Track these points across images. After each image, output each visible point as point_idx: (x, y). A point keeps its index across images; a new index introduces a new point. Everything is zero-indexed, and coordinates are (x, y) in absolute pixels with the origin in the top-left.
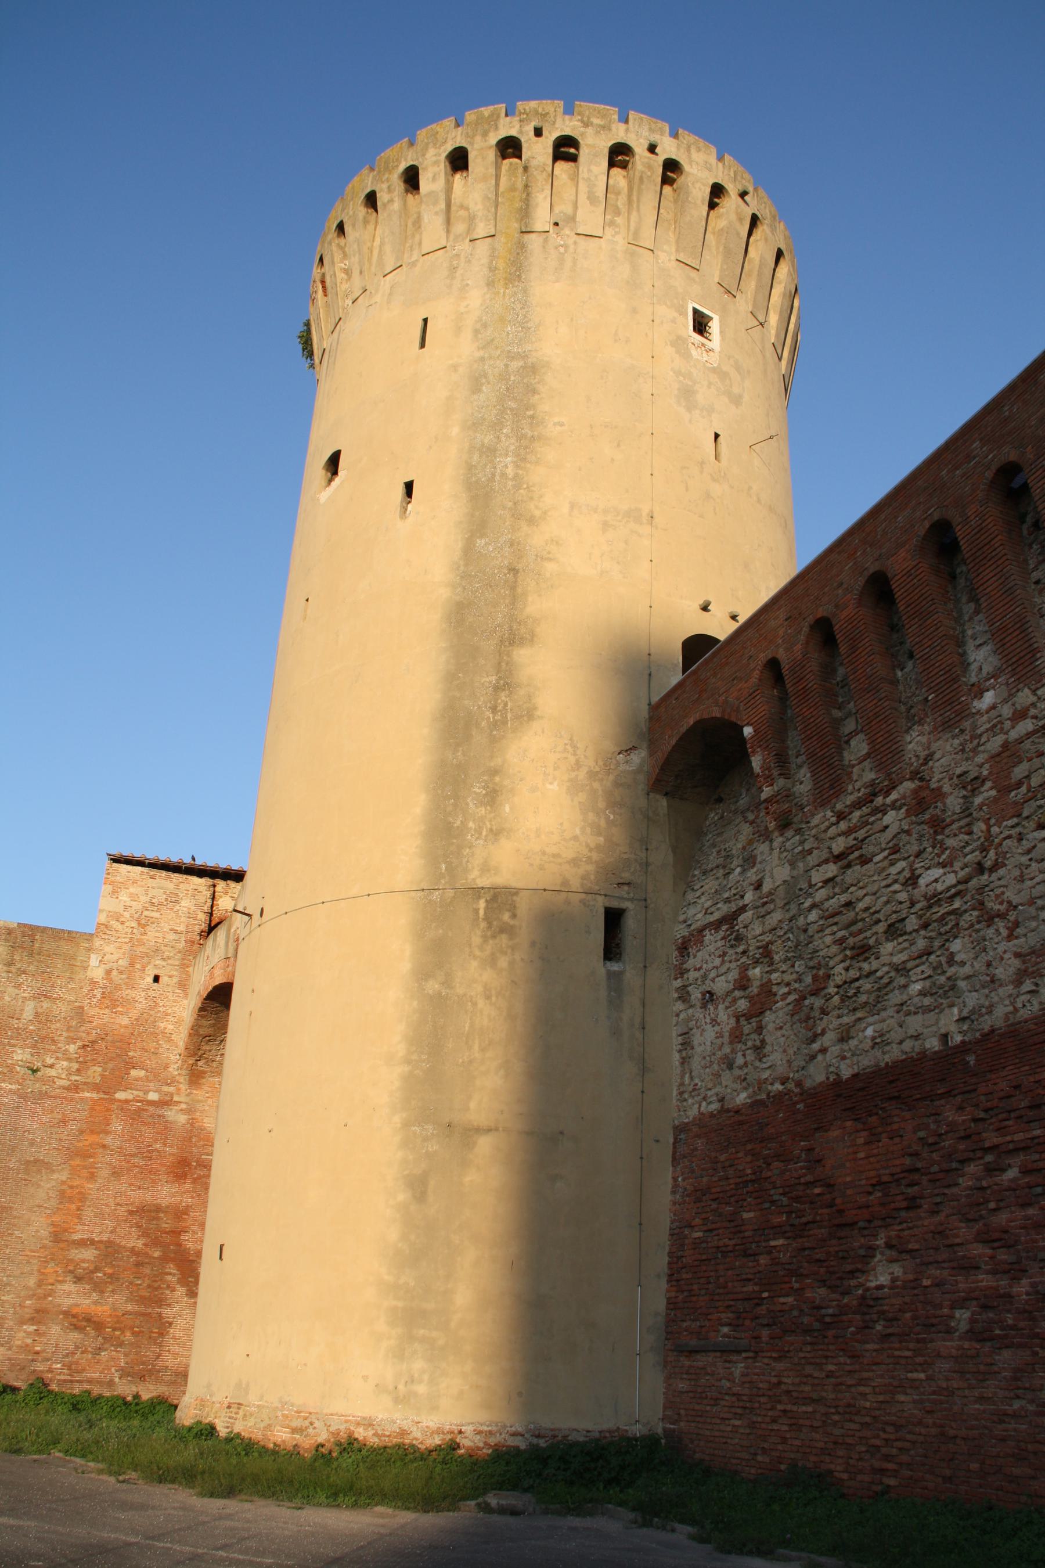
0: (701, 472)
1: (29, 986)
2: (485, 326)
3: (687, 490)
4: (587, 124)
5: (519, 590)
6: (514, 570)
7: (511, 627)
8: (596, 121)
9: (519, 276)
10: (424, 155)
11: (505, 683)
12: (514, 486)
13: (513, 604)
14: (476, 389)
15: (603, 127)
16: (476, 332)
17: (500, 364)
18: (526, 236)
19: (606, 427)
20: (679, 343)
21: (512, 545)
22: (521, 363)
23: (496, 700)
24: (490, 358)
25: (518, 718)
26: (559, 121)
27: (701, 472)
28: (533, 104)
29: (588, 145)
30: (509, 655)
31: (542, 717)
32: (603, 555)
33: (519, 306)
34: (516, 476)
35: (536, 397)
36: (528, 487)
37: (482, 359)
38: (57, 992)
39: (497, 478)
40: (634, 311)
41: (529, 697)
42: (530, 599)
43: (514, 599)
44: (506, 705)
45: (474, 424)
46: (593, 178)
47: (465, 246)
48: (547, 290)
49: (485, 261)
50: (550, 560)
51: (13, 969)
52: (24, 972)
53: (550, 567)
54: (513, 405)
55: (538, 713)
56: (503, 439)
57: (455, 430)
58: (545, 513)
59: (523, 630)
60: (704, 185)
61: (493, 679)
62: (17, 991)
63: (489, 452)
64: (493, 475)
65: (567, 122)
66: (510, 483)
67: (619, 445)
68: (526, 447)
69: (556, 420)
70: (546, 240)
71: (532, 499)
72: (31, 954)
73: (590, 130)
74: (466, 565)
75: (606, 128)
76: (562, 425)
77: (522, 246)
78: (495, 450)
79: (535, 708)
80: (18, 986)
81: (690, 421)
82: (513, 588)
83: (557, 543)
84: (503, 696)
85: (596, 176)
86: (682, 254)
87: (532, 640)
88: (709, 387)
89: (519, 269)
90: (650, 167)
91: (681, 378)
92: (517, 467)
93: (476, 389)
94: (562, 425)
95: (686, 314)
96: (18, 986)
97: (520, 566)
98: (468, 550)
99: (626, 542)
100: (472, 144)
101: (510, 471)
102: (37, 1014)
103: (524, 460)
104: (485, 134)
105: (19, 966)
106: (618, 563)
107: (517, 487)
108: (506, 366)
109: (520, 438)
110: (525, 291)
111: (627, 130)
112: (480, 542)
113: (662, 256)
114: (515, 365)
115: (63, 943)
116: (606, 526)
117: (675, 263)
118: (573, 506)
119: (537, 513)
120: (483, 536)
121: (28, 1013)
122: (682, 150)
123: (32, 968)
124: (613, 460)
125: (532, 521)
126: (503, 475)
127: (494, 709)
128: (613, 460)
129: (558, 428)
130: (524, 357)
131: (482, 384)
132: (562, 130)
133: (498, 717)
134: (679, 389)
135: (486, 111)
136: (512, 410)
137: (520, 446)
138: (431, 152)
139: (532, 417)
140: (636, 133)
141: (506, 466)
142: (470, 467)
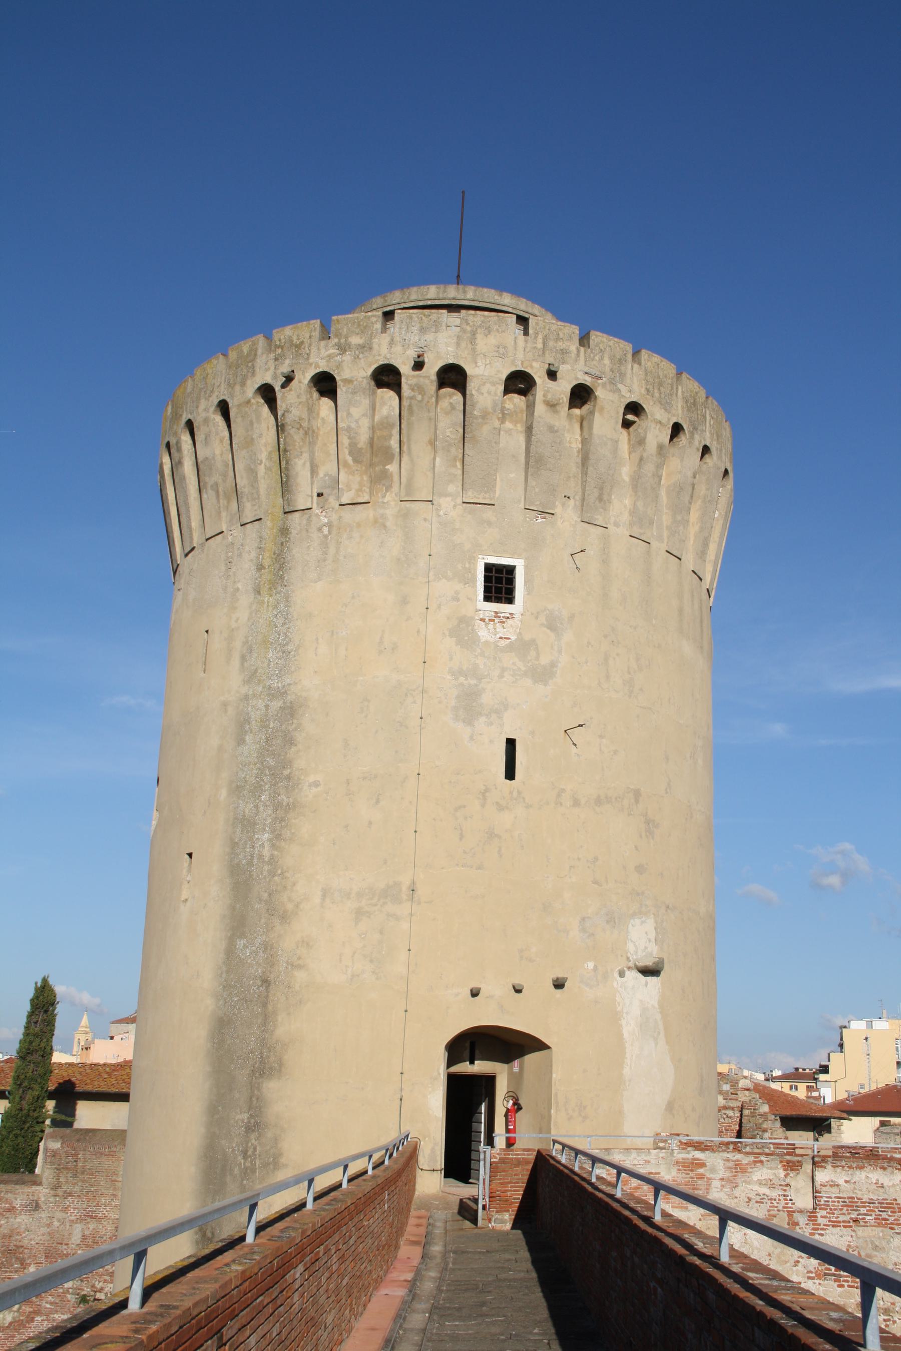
0: (483, 806)
1: (75, 1207)
2: (250, 650)
3: (461, 837)
4: (343, 349)
5: (270, 1007)
6: (266, 982)
7: (261, 1053)
8: (355, 340)
9: (282, 578)
10: (197, 407)
11: (254, 1126)
12: (269, 871)
13: (264, 1025)
14: (241, 741)
16: (243, 658)
17: (261, 704)
18: (290, 516)
19: (364, 778)
20: (462, 631)
21: (266, 949)
22: (280, 704)
23: (247, 1143)
24: (254, 695)
25: (265, 1165)
26: (314, 349)
27: (483, 806)
29: (348, 381)
30: (259, 1089)
31: (285, 1166)
32: (354, 953)
33: (281, 620)
34: (272, 857)
35: (293, 749)
36: (282, 873)
37: (246, 698)
38: (102, 1211)
39: (255, 860)
40: (404, 601)
41: (276, 1140)
42: (280, 1018)
43: (266, 1017)
44: (255, 1149)
45: (238, 787)
46: (353, 425)
47: (237, 531)
48: (309, 592)
49: (253, 554)
50: (300, 967)
51: (60, 1192)
52: (70, 1194)
53: (300, 976)
54: (271, 762)
55: (283, 1160)
56: (262, 808)
57: (223, 793)
58: (297, 906)
59: (272, 1059)
60: (493, 384)
61: (245, 1116)
62: (64, 1215)
63: (248, 824)
64: (252, 856)
65: (323, 351)
66: (266, 868)
67: (378, 801)
68: (282, 820)
69: (312, 779)
70: (309, 520)
71: (285, 888)
72: (75, 1176)
73: (347, 357)
74: (228, 972)
75: (366, 348)
76: (316, 784)
77: (284, 531)
78: (255, 824)
79: (281, 1155)
80: (65, 1209)
81: (471, 738)
82: (265, 1005)
83: (308, 944)
84: (253, 1136)
85: (357, 422)
86: (470, 493)
87: (280, 1071)
88: (501, 676)
89: (281, 568)
90: (419, 389)
91: (462, 679)
92: (273, 846)
93: (241, 741)
94: (316, 784)
95: (474, 580)
96: (65, 1209)
97: (272, 977)
98: (230, 951)
99: (381, 932)
100: (232, 396)
101: (266, 852)
102: (84, 1237)
103: (279, 837)
104: (243, 384)
105: (65, 1188)
106: (371, 961)
107: (272, 874)
108: (267, 706)
109: (277, 806)
110: (287, 599)
111: (392, 342)
112: (240, 943)
113: (445, 503)
114: (276, 704)
115: (104, 1158)
116: (359, 914)
117: (460, 508)
118: (325, 893)
119: (290, 906)
120: (242, 936)
121: (76, 1238)
122: (463, 345)
123: (77, 1189)
124: (370, 823)
125: (285, 918)
126: (261, 856)
127: (245, 1154)
128: (370, 823)
129: (314, 790)
130: (282, 693)
131: (246, 732)
132: (317, 366)
133: (248, 1164)
134: (458, 697)
135: (245, 347)
136: (270, 769)
137: (276, 818)
138: (203, 404)
139: (288, 778)
141: (263, 845)
142: (234, 845)
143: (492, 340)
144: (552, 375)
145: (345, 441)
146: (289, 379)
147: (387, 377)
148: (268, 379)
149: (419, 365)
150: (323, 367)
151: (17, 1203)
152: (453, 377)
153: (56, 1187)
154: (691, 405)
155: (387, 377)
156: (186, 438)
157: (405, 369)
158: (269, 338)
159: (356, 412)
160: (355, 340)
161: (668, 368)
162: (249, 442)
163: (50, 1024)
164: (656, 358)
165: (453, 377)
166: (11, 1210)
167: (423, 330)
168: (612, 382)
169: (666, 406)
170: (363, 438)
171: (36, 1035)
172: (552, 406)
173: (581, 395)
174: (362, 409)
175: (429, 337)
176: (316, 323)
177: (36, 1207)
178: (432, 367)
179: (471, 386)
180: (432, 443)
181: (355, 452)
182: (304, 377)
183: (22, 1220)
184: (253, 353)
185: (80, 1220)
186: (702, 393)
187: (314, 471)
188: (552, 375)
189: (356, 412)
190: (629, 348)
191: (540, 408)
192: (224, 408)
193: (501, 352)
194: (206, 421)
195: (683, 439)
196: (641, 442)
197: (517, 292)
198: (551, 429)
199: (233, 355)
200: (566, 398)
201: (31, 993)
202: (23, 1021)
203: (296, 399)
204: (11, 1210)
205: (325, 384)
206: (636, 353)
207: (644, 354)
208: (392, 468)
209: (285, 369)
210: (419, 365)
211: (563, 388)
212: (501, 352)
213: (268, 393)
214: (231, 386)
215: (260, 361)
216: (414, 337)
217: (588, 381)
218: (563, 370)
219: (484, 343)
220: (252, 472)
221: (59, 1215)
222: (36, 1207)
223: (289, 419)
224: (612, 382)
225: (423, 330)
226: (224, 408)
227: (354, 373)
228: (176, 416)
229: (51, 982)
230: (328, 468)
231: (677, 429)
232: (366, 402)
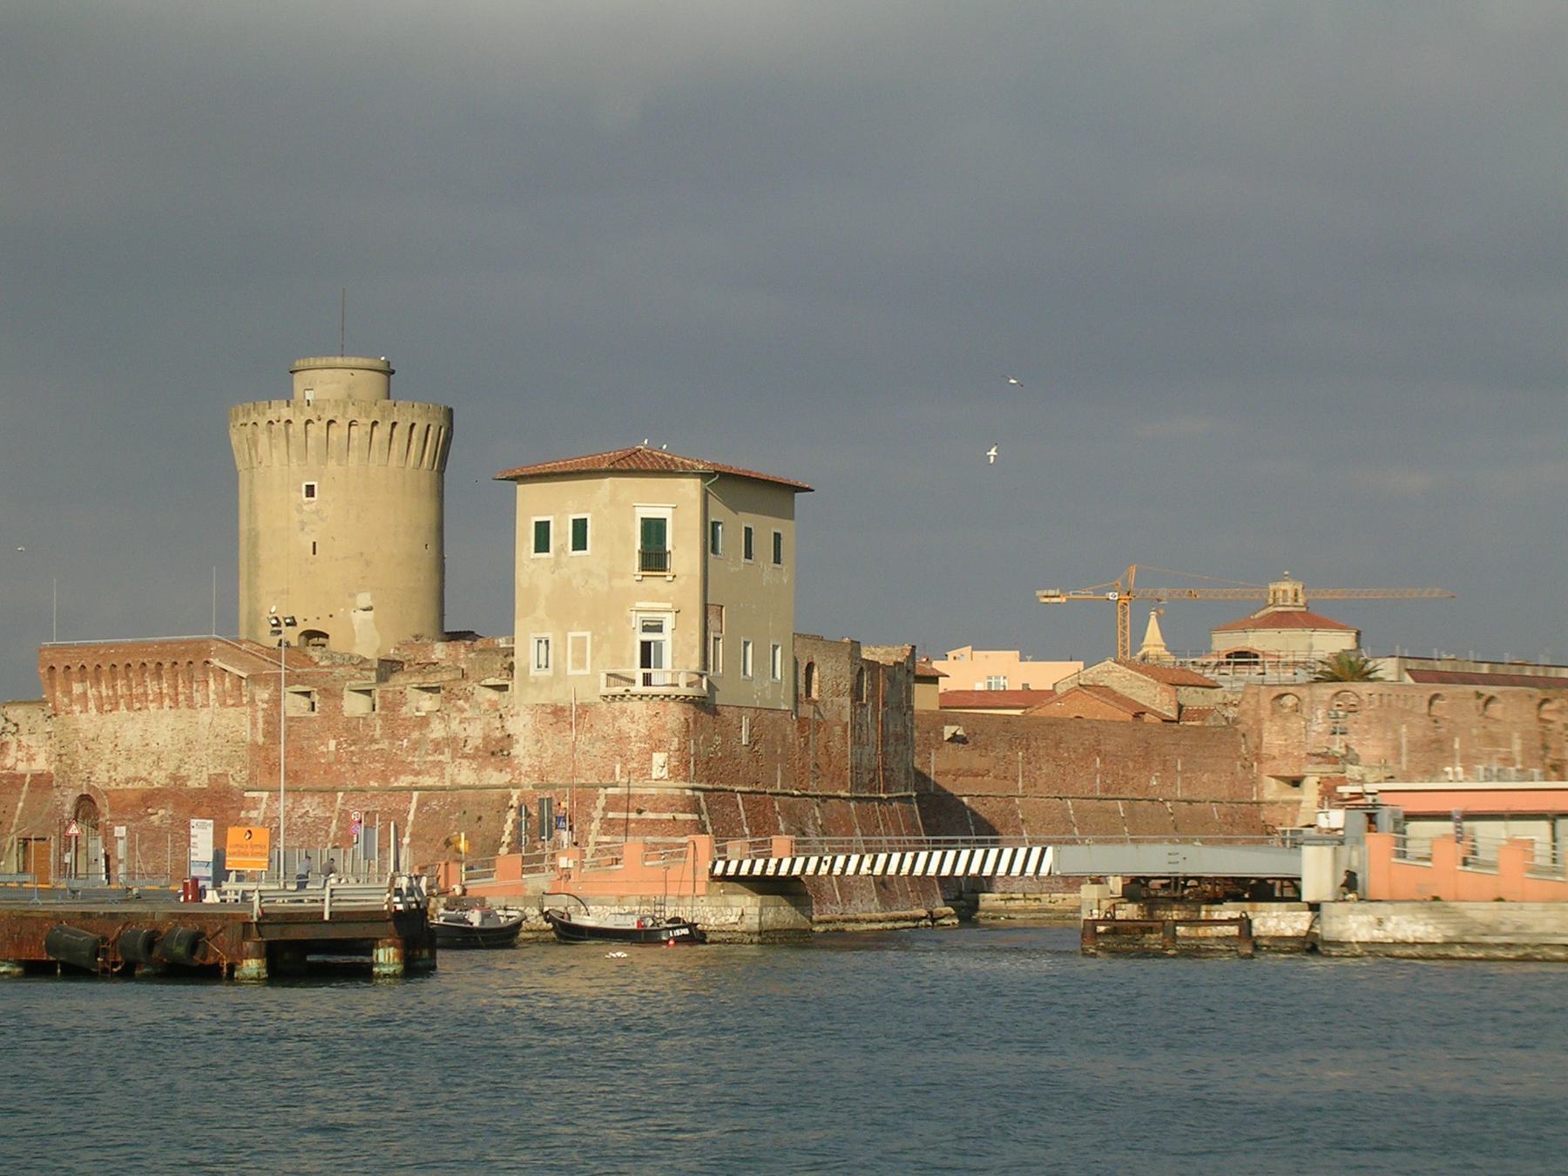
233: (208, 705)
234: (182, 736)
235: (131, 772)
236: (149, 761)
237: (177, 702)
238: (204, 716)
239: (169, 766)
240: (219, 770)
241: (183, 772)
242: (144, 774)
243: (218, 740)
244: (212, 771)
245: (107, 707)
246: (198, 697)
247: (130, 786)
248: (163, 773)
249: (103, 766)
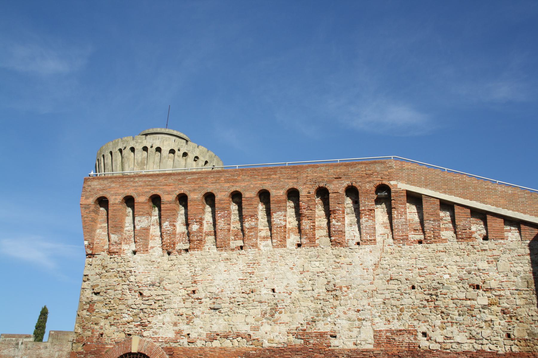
1: (57, 348)
4: (137, 142)
15: (141, 142)
28: (126, 138)
38: (64, 349)
72: (57, 340)
73: (137, 144)
80: (54, 348)
90: (152, 151)
96: (54, 348)
140: (148, 142)
143: (167, 143)
144: (179, 150)
145: (136, 161)
146: (125, 148)
147: (145, 149)
148: (121, 148)
149: (152, 147)
150: (132, 146)
151: (41, 347)
152: (159, 150)
153: (52, 343)
154: (211, 157)
155: (145, 149)
156: (102, 158)
157: (149, 147)
158: (122, 139)
159: (138, 155)
160: (139, 141)
161: (205, 149)
162: (116, 160)
163: (46, 319)
164: (203, 147)
165: (159, 150)
166: (40, 348)
167: (153, 140)
168: (192, 152)
169: (204, 157)
170: (140, 161)
171: (41, 322)
172: (179, 156)
173: (185, 154)
174: (140, 155)
175: (154, 141)
176: (132, 137)
177: (46, 348)
178: (154, 148)
179: (162, 152)
180: (154, 163)
181: (138, 164)
182: (128, 148)
183: (42, 351)
184: (118, 142)
185: (58, 351)
186: (214, 155)
187: (129, 167)
188: (179, 150)
189: (138, 155)
190: (197, 145)
191: (176, 157)
192: (111, 153)
193: (169, 145)
194: (107, 155)
195: (208, 164)
196: (198, 164)
197: (178, 130)
198: (178, 161)
199: (114, 142)
200: (182, 155)
201: (41, 310)
202: (38, 318)
203: (127, 152)
204: (40, 348)
205: (133, 149)
206: (198, 147)
207: (200, 146)
208: (145, 167)
209: (124, 146)
210: (152, 147)
211: (181, 153)
212: (169, 145)
213: (121, 151)
214: (113, 148)
215: (119, 144)
216: (151, 141)
217: (187, 151)
218: (181, 149)
219: (165, 143)
220: (116, 166)
221: (52, 350)
222: (46, 348)
223: (125, 156)
224: (192, 152)
225: (153, 140)
226: (111, 153)
227: (139, 148)
228: (100, 153)
229: (47, 307)
230: (132, 166)
231: (206, 162)
232: (141, 154)
233: (373, 241)
234: (322, 281)
235: (219, 324)
236: (257, 311)
237: (312, 241)
238: (367, 255)
239: (299, 319)
240: (396, 325)
241: (322, 327)
242: (244, 329)
243: (393, 285)
244: (381, 326)
245: (180, 246)
246: (351, 232)
247: (216, 344)
248: (284, 329)
249: (169, 317)
